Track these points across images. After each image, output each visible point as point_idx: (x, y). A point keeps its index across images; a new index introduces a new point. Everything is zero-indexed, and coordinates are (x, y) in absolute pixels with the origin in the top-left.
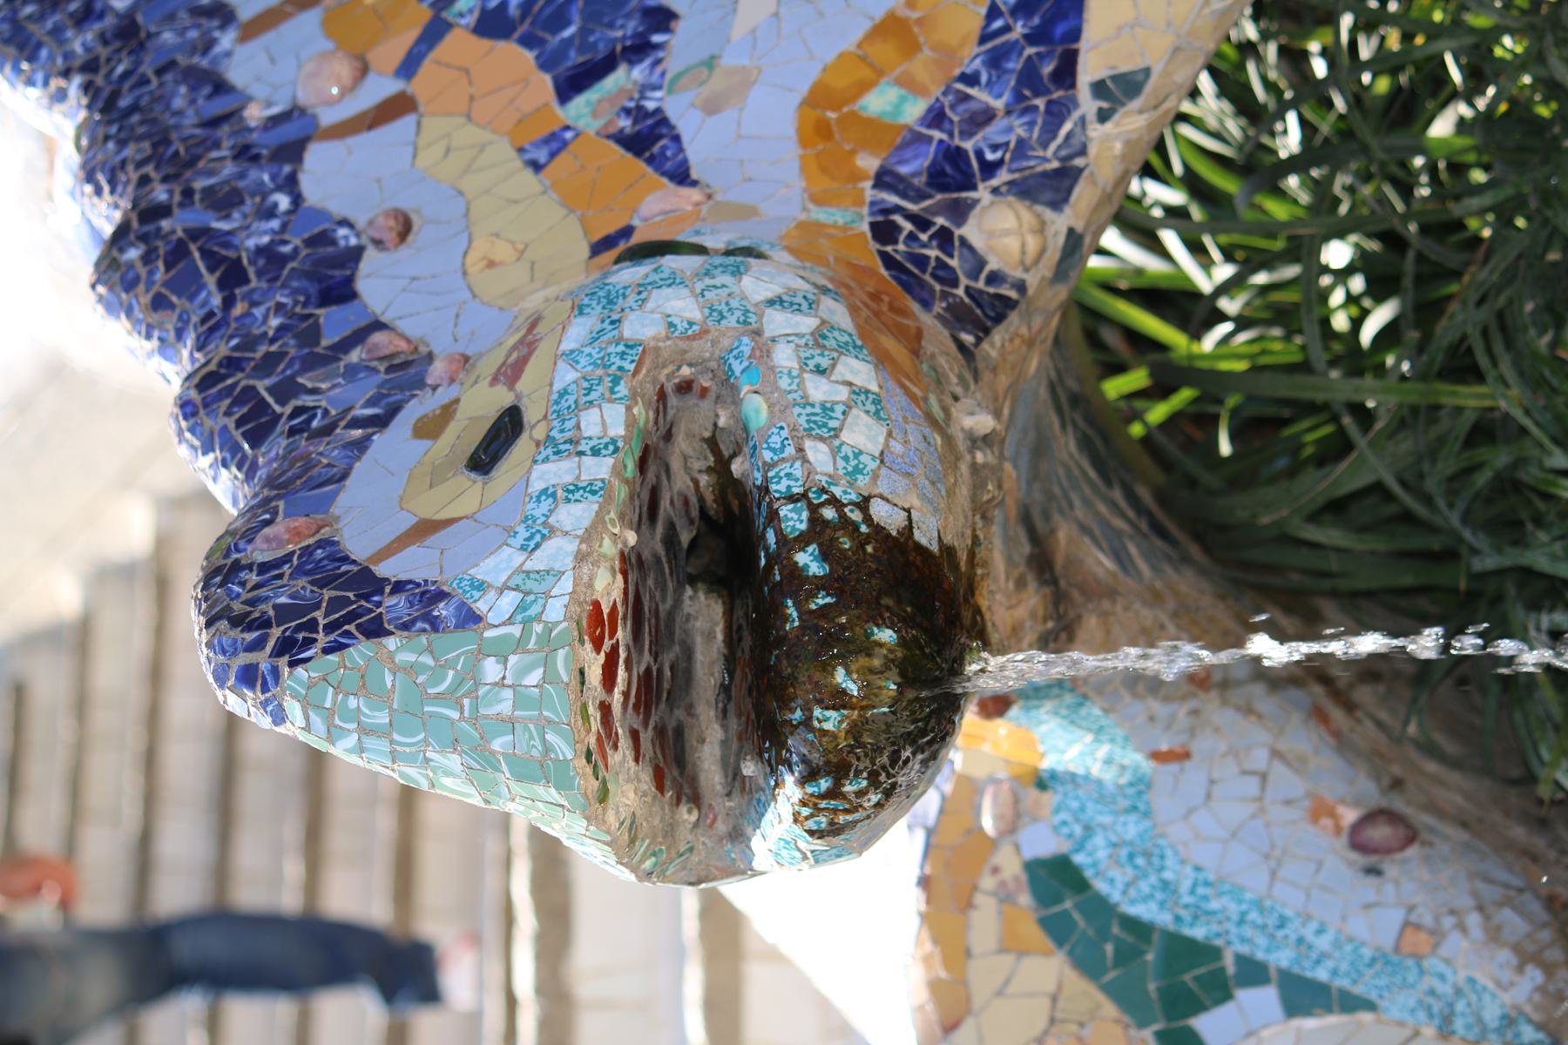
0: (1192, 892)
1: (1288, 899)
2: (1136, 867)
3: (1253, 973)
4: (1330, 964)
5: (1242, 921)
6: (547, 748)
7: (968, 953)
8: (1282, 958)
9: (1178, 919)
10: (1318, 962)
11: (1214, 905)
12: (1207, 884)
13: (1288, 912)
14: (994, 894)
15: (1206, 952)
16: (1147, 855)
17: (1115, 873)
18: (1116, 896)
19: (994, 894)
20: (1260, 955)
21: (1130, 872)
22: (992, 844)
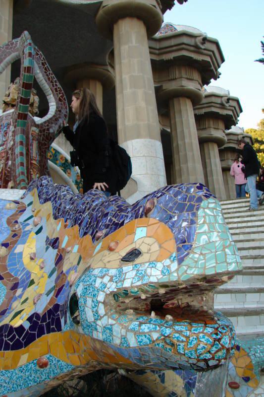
6: (230, 264)
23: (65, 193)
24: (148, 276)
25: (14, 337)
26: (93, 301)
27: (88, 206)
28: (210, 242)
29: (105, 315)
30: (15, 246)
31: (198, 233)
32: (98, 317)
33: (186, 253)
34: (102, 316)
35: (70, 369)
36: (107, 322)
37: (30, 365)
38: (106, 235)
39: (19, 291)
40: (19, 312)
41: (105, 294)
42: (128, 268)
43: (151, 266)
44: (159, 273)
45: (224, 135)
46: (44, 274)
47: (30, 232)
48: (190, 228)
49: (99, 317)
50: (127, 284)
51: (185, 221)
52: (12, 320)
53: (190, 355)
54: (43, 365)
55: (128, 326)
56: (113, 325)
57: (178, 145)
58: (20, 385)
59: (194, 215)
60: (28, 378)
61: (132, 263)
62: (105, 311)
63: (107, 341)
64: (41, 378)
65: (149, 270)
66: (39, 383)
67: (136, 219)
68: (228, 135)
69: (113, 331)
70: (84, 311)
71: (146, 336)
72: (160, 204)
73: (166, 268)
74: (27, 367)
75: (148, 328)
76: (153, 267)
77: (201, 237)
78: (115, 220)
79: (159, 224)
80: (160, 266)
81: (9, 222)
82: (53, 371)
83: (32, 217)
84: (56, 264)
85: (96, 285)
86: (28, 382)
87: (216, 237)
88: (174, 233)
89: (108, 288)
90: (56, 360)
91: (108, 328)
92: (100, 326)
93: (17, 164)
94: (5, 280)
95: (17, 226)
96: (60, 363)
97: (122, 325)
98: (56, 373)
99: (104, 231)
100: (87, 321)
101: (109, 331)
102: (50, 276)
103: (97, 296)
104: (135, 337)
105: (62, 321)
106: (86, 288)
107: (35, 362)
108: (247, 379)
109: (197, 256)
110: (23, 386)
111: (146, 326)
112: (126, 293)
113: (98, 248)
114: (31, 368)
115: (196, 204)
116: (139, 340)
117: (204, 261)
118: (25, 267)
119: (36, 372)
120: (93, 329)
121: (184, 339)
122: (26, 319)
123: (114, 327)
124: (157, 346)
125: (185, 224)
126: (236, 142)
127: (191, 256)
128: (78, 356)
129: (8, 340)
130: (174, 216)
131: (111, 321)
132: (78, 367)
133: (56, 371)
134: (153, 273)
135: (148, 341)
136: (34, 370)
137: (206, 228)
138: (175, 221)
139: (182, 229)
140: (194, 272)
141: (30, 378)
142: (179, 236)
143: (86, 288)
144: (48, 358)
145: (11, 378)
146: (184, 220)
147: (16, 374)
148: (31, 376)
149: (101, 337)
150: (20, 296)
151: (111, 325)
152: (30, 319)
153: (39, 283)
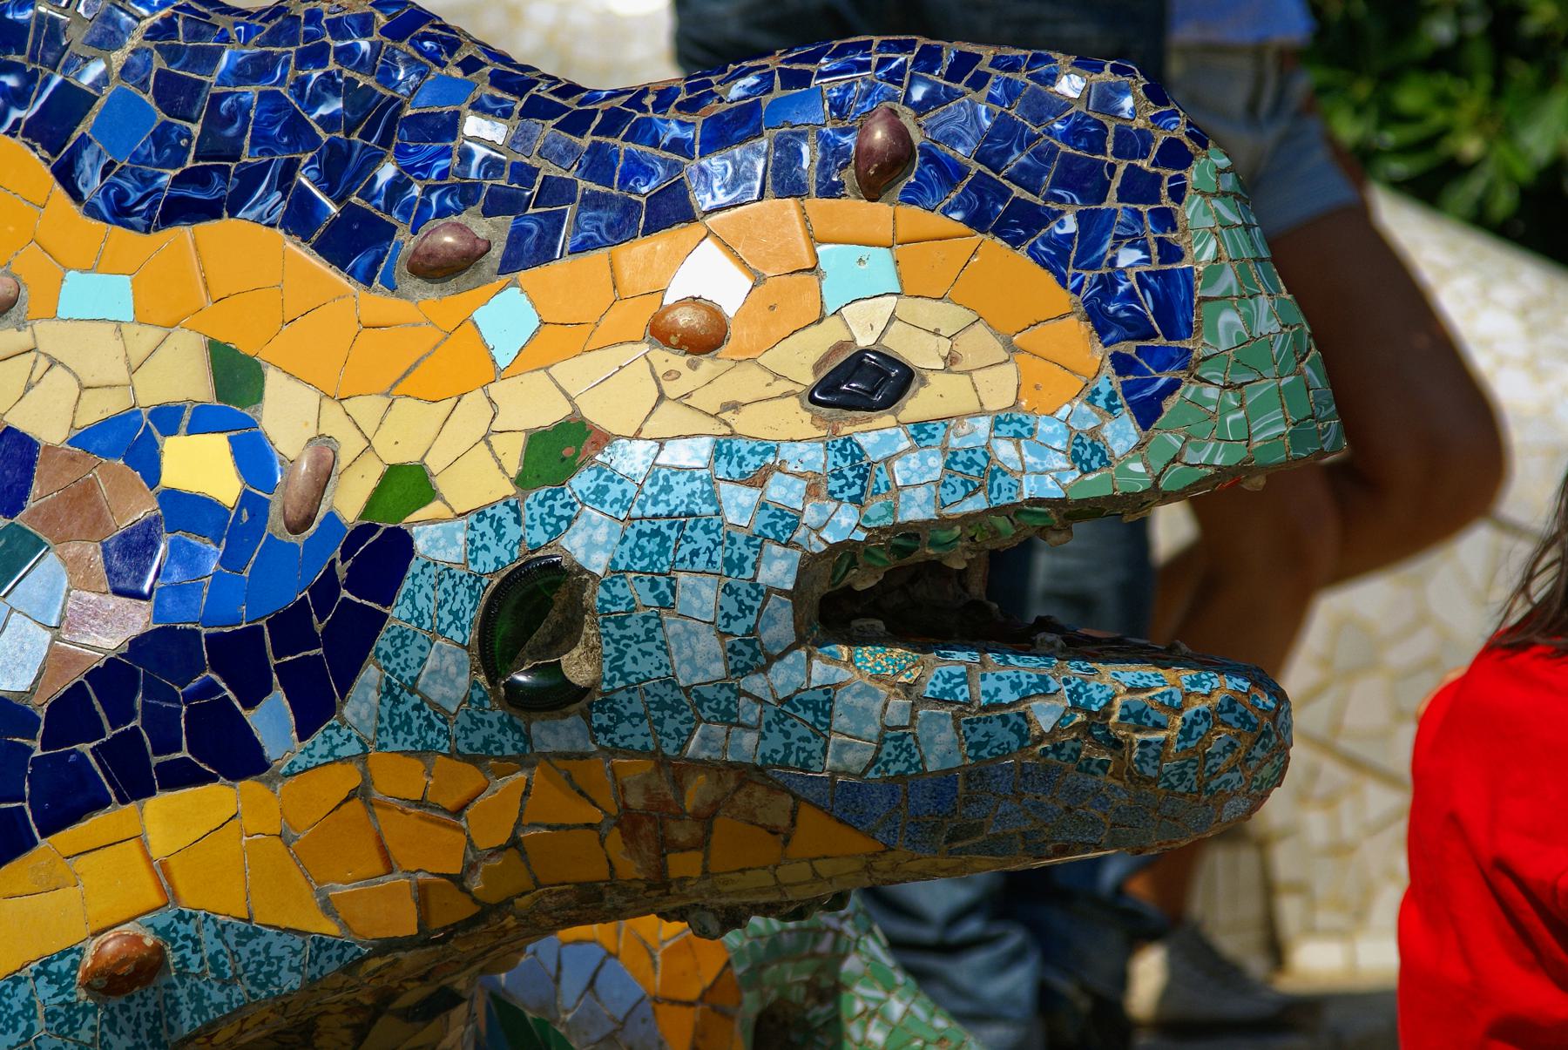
26: (729, 590)
32: (754, 658)
33: (1164, 379)
34: (778, 651)
36: (799, 679)
37: (23, 991)
41: (798, 554)
44: (1059, 462)
49: (762, 660)
50: (916, 509)
51: (1131, 246)
53: (1174, 780)
56: (837, 686)
59: (1165, 219)
61: (885, 420)
63: (784, 764)
65: (1005, 451)
69: (837, 712)
70: (650, 638)
73: (1087, 441)
75: (1015, 686)
76: (1018, 435)
87: (1269, 319)
89: (817, 530)
91: (805, 704)
92: (758, 700)
98: (219, 1007)
100: (669, 681)
101: (809, 717)
103: (755, 567)
106: (657, 532)
107: (65, 964)
109: (1211, 393)
111: (999, 678)
114: (29, 1004)
116: (975, 738)
117: (1241, 414)
123: (844, 698)
124: (1051, 756)
125: (1128, 257)
127: (1188, 390)
131: (820, 671)
133: (218, 997)
135: (1013, 737)
137: (1229, 280)
138: (1069, 238)
139: (1119, 278)
142: (1111, 309)
143: (657, 532)
144: (164, 932)
151: (830, 690)
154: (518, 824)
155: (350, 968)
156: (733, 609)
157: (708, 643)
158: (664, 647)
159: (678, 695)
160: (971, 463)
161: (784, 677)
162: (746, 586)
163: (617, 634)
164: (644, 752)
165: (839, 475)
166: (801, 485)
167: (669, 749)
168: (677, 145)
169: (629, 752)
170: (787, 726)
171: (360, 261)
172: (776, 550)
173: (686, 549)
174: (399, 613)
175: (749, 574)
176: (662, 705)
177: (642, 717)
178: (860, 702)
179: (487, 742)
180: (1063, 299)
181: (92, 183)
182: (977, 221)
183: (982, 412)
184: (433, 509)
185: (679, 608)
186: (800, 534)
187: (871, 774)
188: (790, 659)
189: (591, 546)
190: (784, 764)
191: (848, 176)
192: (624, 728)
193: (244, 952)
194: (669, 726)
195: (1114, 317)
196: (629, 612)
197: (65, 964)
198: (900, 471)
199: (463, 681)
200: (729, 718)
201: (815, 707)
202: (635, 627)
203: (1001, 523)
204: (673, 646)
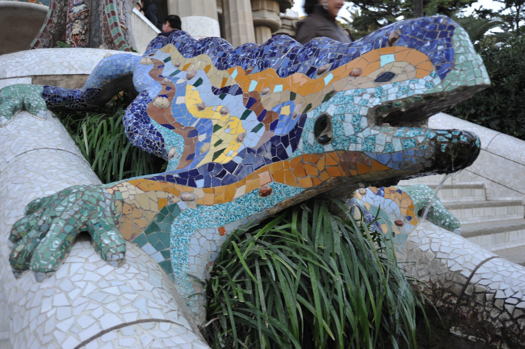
0: (182, 239)
1: (191, 260)
2: (184, 226)
3: (166, 254)
4: (179, 271)
5: (180, 251)
6: (485, 78)
7: (156, 191)
8: (174, 261)
9: (174, 237)
10: (178, 269)
11: (181, 244)
12: (186, 242)
13: (188, 261)
14: (168, 197)
15: (168, 244)
16: (188, 229)
17: (180, 223)
18: (175, 223)
19: (168, 197)
20: (172, 256)
21: (183, 225)
22: (178, 196)
23: (225, 44)
24: (412, 90)
25: (224, 173)
26: (354, 116)
27: (283, 49)
28: (467, 61)
29: (367, 127)
30: (174, 97)
31: (456, 54)
32: (359, 129)
33: (447, 70)
35: (299, 192)
36: (369, 134)
37: (250, 195)
38: (333, 68)
39: (202, 138)
40: (222, 151)
41: (367, 108)
42: (385, 86)
43: (412, 82)
44: (423, 87)
45: (279, 18)
46: (232, 118)
47: (184, 85)
48: (448, 50)
49: (361, 130)
50: (392, 98)
52: (214, 159)
54: (266, 193)
55: (393, 133)
57: (230, 27)
58: (239, 216)
59: (449, 40)
60: (248, 207)
61: (389, 82)
62: (368, 123)
63: (367, 151)
64: (263, 206)
65: (412, 86)
66: (261, 211)
67: (377, 50)
68: (283, 18)
69: (377, 139)
71: (411, 141)
72: (406, 33)
74: (245, 197)
75: (414, 134)
77: (459, 57)
78: (341, 54)
79: (408, 51)
80: (422, 81)
81: (151, 74)
82: (278, 197)
83: (177, 72)
84: (248, 106)
85: (356, 102)
86: (248, 212)
88: (429, 56)
89: (371, 103)
90: (282, 186)
91: (370, 138)
93: (110, 25)
94: (176, 129)
95: (166, 80)
96: (286, 188)
97: (387, 134)
99: (329, 66)
100: (344, 135)
101: (371, 141)
102: (244, 116)
103: (359, 111)
104: (401, 142)
105: (289, 150)
107: (256, 191)
108: (409, 218)
109: (457, 72)
110: (242, 216)
112: (390, 104)
113: (328, 78)
114: (251, 198)
115: (449, 31)
116: (405, 144)
118: (194, 116)
119: (257, 201)
120: (352, 141)
121: (447, 140)
122: (236, 153)
123: (378, 137)
125: (440, 48)
126: (289, 28)
127: (452, 72)
128: (312, 179)
129: (217, 176)
130: (426, 43)
131: (373, 132)
132: (308, 189)
133: (281, 197)
134: (417, 87)
135: (413, 145)
136: (254, 200)
138: (428, 46)
140: (457, 84)
141: (250, 207)
144: (272, 186)
145: (226, 211)
146: (438, 45)
147: (233, 206)
148: (251, 206)
149: (359, 148)
150: (208, 140)
151: (374, 135)
152: (241, 154)
153: (228, 127)
154: (325, 166)
155: (303, 193)
156: (355, 119)
157: (351, 127)
158: (343, 129)
159: (346, 138)
160: (404, 89)
161: (366, 133)
162: (357, 115)
163: (335, 127)
164: (342, 150)
165: (377, 93)
166: (369, 96)
167: (346, 149)
168: (360, 46)
169: (339, 150)
170: (367, 143)
171: (311, 75)
172: (363, 108)
173: (347, 109)
174: (304, 128)
175: (358, 112)
176: (344, 140)
177: (341, 143)
178: (381, 138)
179: (318, 150)
180: (426, 58)
181: (280, 72)
182: (411, 46)
183: (408, 79)
184: (311, 109)
185: (346, 121)
186: (368, 105)
187: (384, 152)
188: (367, 129)
189: (331, 111)
190: (367, 151)
191: (387, 43)
192: (338, 145)
193: (285, 190)
194: (345, 144)
195: (437, 60)
196: (337, 122)
197: (256, 191)
198: (390, 92)
199: (313, 139)
200: (356, 142)
201: (372, 139)
202: (338, 125)
203: (410, 99)
204: (345, 128)
